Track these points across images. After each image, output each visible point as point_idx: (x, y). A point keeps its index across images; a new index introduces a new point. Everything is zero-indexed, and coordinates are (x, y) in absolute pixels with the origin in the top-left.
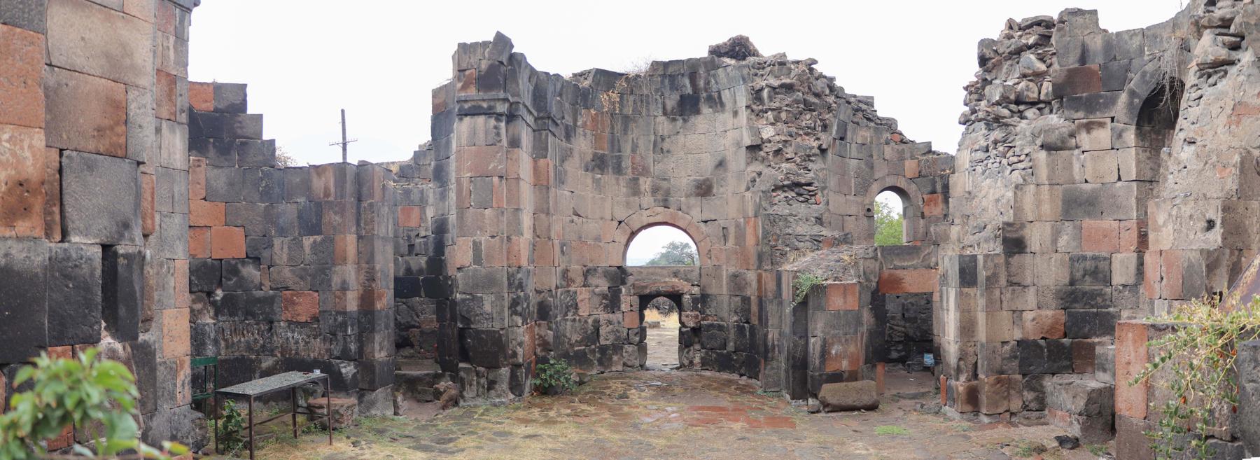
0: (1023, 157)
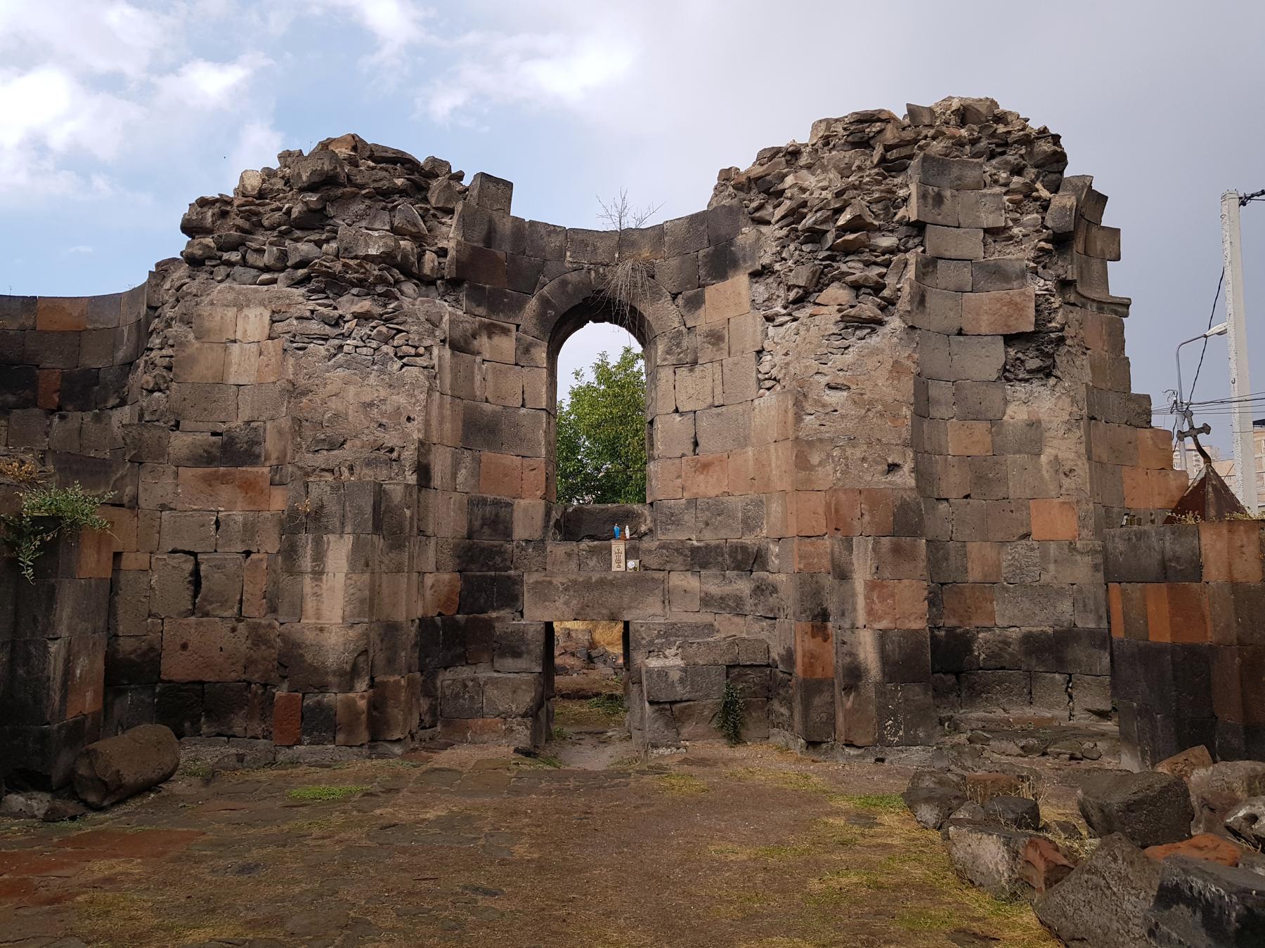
0: (421, 350)
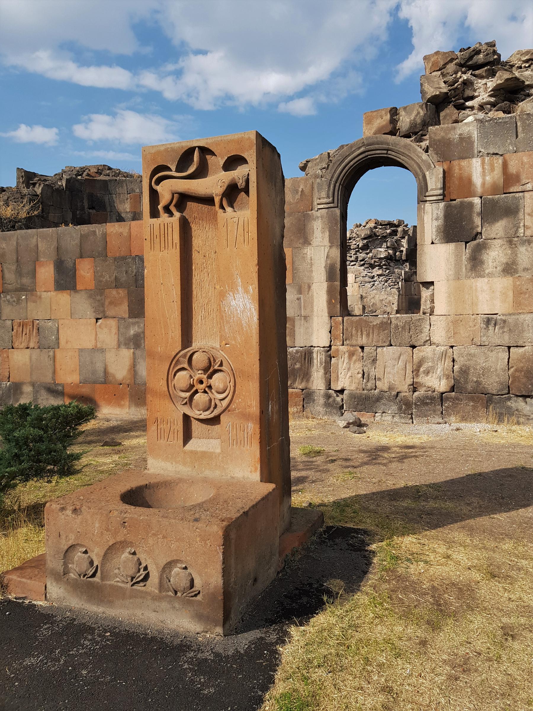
0: (396, 283)
